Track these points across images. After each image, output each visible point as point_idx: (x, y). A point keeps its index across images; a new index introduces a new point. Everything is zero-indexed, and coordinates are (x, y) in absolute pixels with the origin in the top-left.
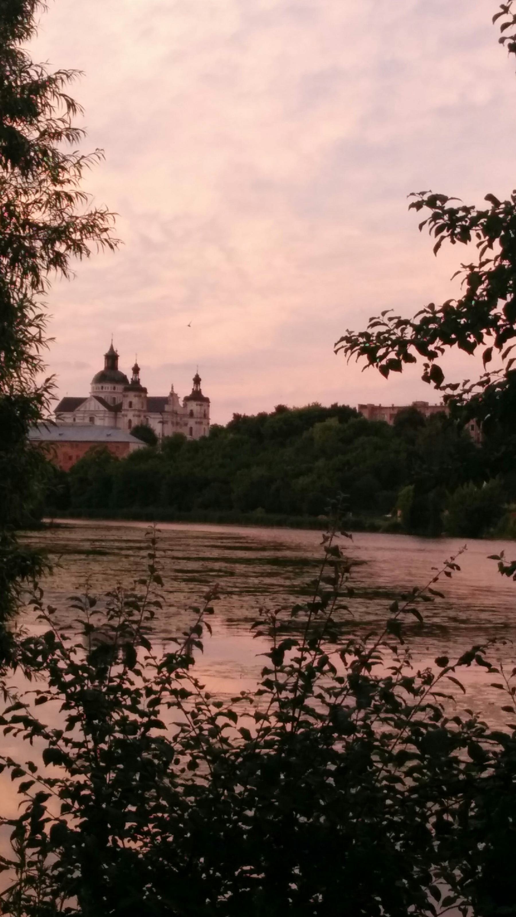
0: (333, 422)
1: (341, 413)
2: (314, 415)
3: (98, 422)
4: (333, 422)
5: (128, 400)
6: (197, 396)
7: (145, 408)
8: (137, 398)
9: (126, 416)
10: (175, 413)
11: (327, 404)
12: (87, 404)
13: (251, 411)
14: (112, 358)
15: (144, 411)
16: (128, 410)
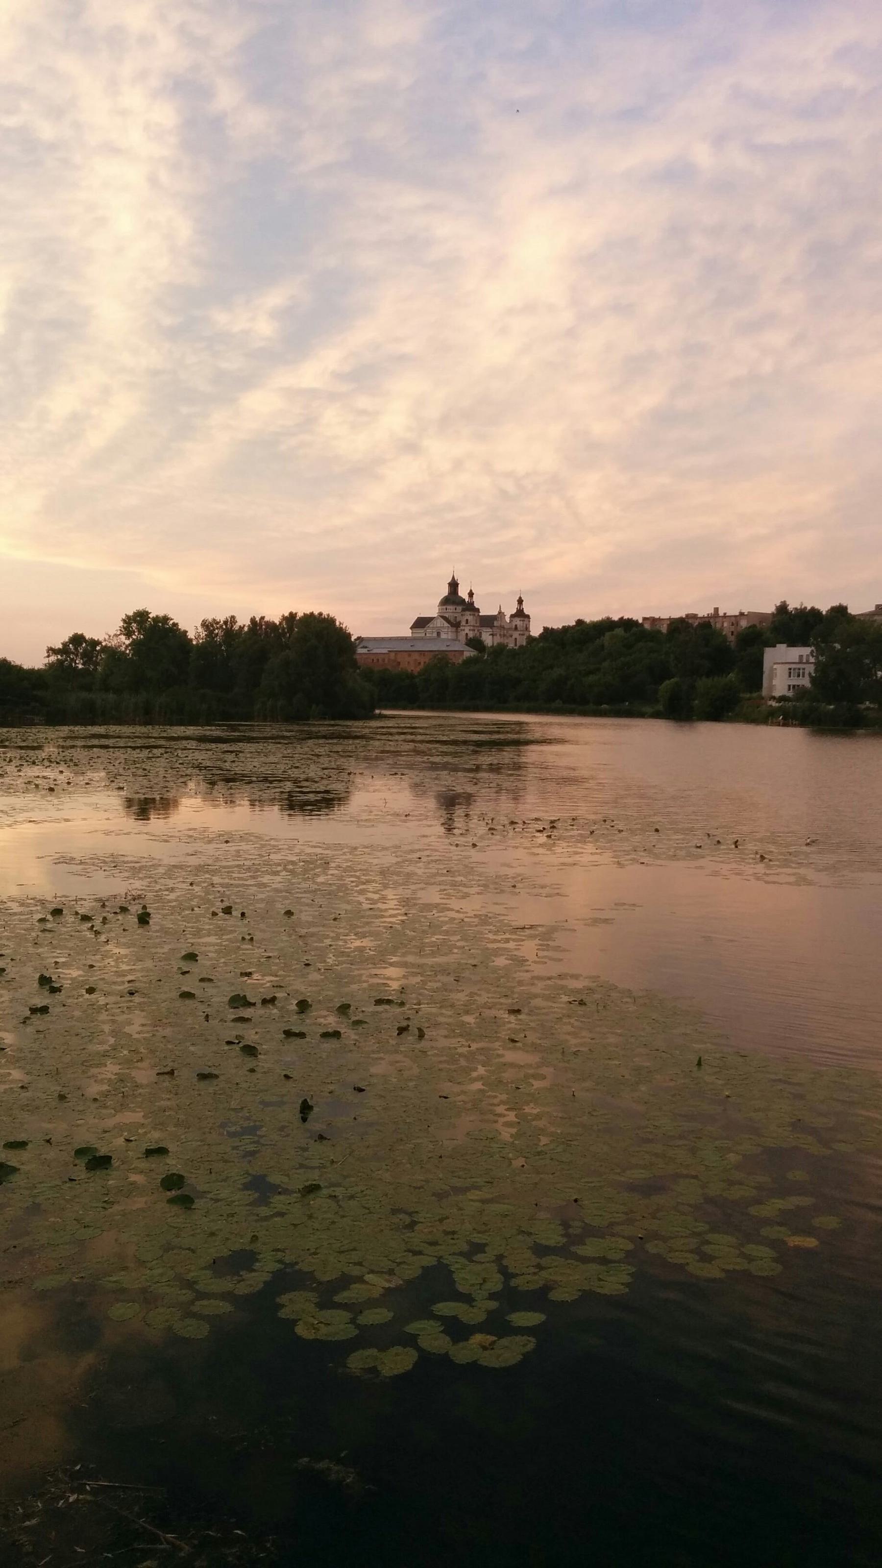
0: (619, 631)
1: (627, 624)
2: (607, 626)
3: (443, 636)
4: (619, 631)
6: (520, 614)
10: (502, 627)
11: (616, 618)
13: (557, 625)
14: (454, 585)
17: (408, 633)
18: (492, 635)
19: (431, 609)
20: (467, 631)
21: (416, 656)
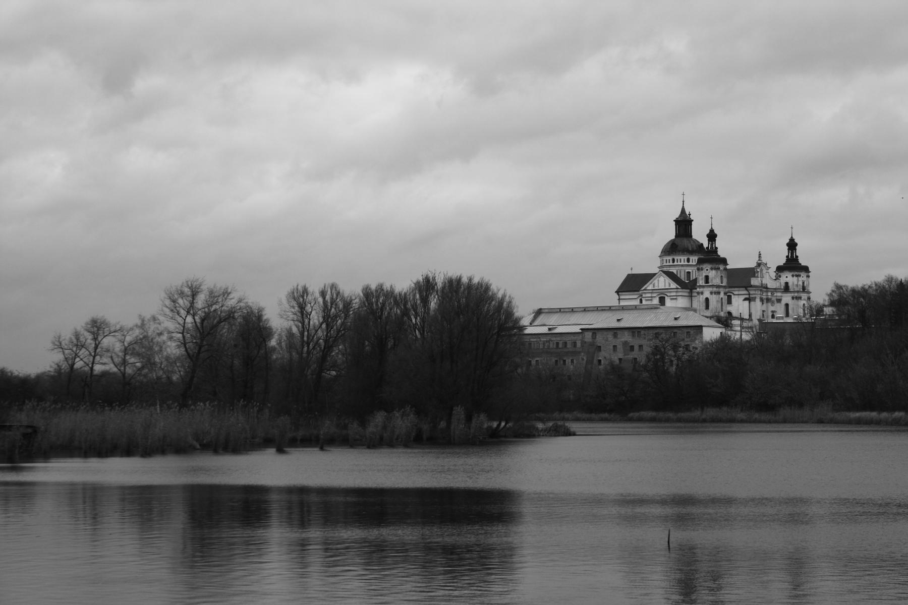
5: (704, 273)
6: (792, 264)
8: (714, 272)
9: (702, 293)
10: (764, 288)
12: (656, 281)
14: (684, 224)
15: (724, 287)
16: (703, 287)
17: (613, 300)
18: (749, 299)
19: (648, 261)
20: (707, 294)
21: (627, 337)
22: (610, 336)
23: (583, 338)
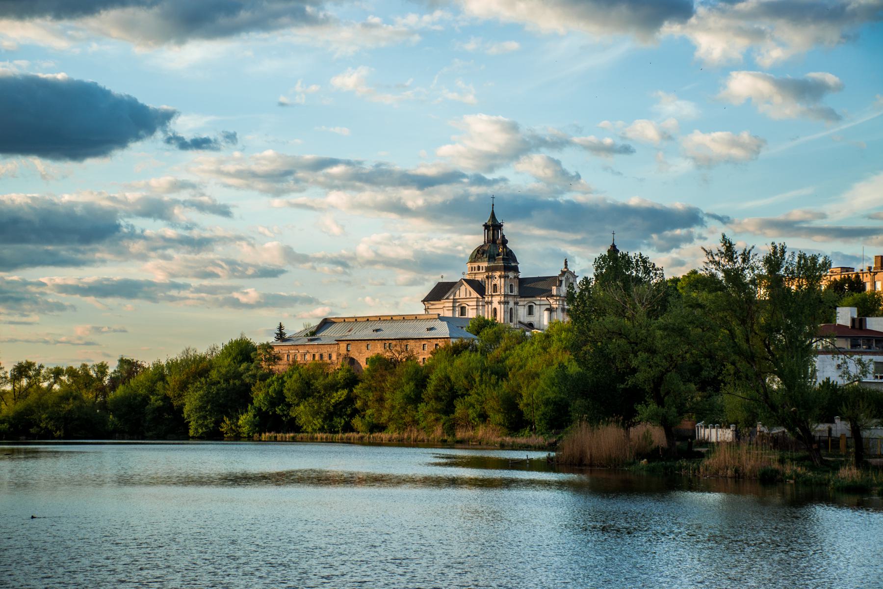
7: (516, 291)
9: (491, 303)
22: (363, 345)
23: (338, 349)
